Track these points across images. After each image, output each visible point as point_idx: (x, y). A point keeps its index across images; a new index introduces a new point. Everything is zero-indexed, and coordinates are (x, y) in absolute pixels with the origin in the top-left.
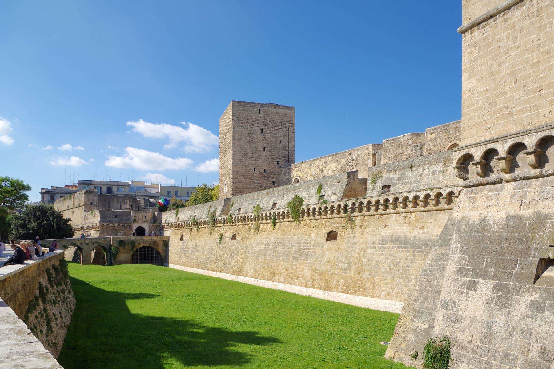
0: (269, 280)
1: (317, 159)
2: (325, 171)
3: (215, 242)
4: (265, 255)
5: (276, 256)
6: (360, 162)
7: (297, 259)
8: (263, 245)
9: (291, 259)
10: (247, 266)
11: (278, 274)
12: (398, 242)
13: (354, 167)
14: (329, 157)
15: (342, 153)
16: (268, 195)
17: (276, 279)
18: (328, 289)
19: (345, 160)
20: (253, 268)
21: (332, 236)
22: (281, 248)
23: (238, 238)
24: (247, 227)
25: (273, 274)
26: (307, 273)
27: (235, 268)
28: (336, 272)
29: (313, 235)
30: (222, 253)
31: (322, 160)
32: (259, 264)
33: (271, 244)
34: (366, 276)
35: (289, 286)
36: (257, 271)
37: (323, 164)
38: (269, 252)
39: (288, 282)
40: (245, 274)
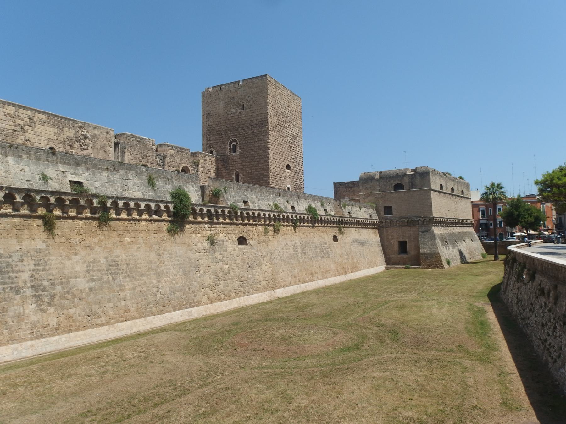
0: (311, 281)
1: (9, 104)
2: (30, 131)
3: (199, 251)
4: (298, 259)
5: (308, 258)
6: (98, 145)
7: (323, 257)
8: (291, 248)
9: (320, 258)
10: (281, 274)
11: (316, 273)
12: (357, 241)
13: (89, 148)
14: (39, 112)
15: (69, 120)
16: (280, 196)
17: (315, 278)
18: (346, 273)
19: (73, 131)
20: (290, 275)
21: (335, 239)
22: (308, 250)
23: (250, 241)
24: (261, 228)
25: (312, 274)
26: (333, 266)
27: (264, 283)
28: (345, 261)
29: (326, 238)
30: (226, 267)
31: (21, 110)
32: (294, 269)
33: (299, 247)
34: (355, 261)
35: (326, 280)
36: (295, 277)
37: (27, 120)
38: (300, 255)
39: (324, 277)
40: (282, 284)
